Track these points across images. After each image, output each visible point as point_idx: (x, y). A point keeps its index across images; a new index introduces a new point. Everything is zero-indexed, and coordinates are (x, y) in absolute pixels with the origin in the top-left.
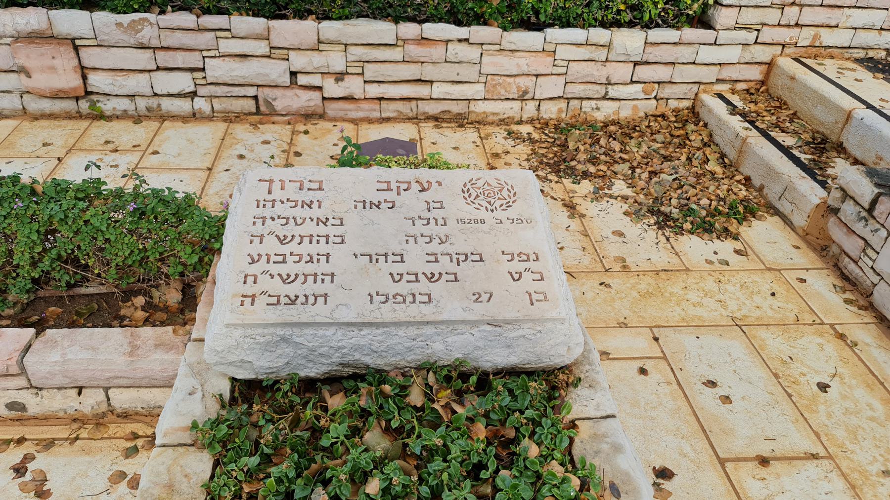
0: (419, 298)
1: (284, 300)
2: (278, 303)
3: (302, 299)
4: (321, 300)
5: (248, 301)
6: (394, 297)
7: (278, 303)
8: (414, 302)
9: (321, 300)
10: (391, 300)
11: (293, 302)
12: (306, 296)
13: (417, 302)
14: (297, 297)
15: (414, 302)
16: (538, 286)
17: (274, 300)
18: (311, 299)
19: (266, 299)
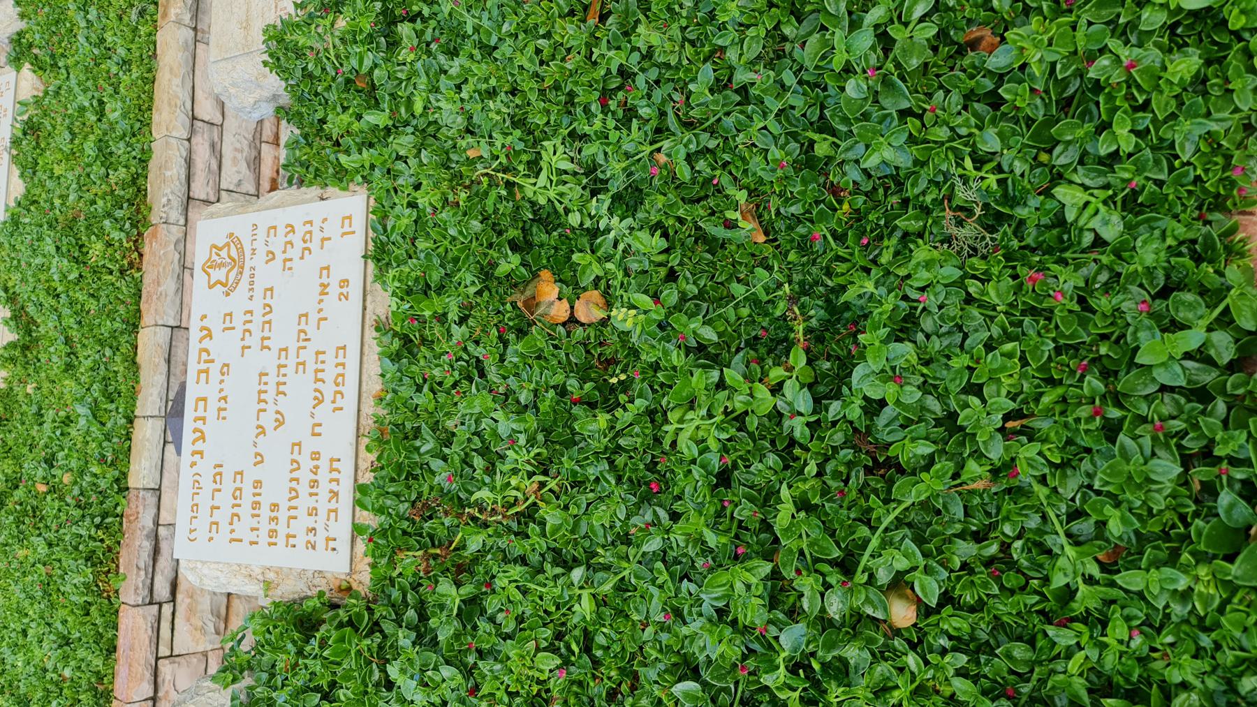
0: (340, 360)
1: (333, 505)
2: (335, 511)
3: (334, 486)
4: (335, 465)
5: (332, 544)
6: (337, 385)
7: (335, 511)
8: (343, 365)
9: (335, 465)
10: (340, 388)
11: (336, 494)
12: (331, 481)
13: (342, 360)
14: (331, 491)
15: (343, 365)
17: (333, 514)
18: (335, 475)
19: (331, 522)
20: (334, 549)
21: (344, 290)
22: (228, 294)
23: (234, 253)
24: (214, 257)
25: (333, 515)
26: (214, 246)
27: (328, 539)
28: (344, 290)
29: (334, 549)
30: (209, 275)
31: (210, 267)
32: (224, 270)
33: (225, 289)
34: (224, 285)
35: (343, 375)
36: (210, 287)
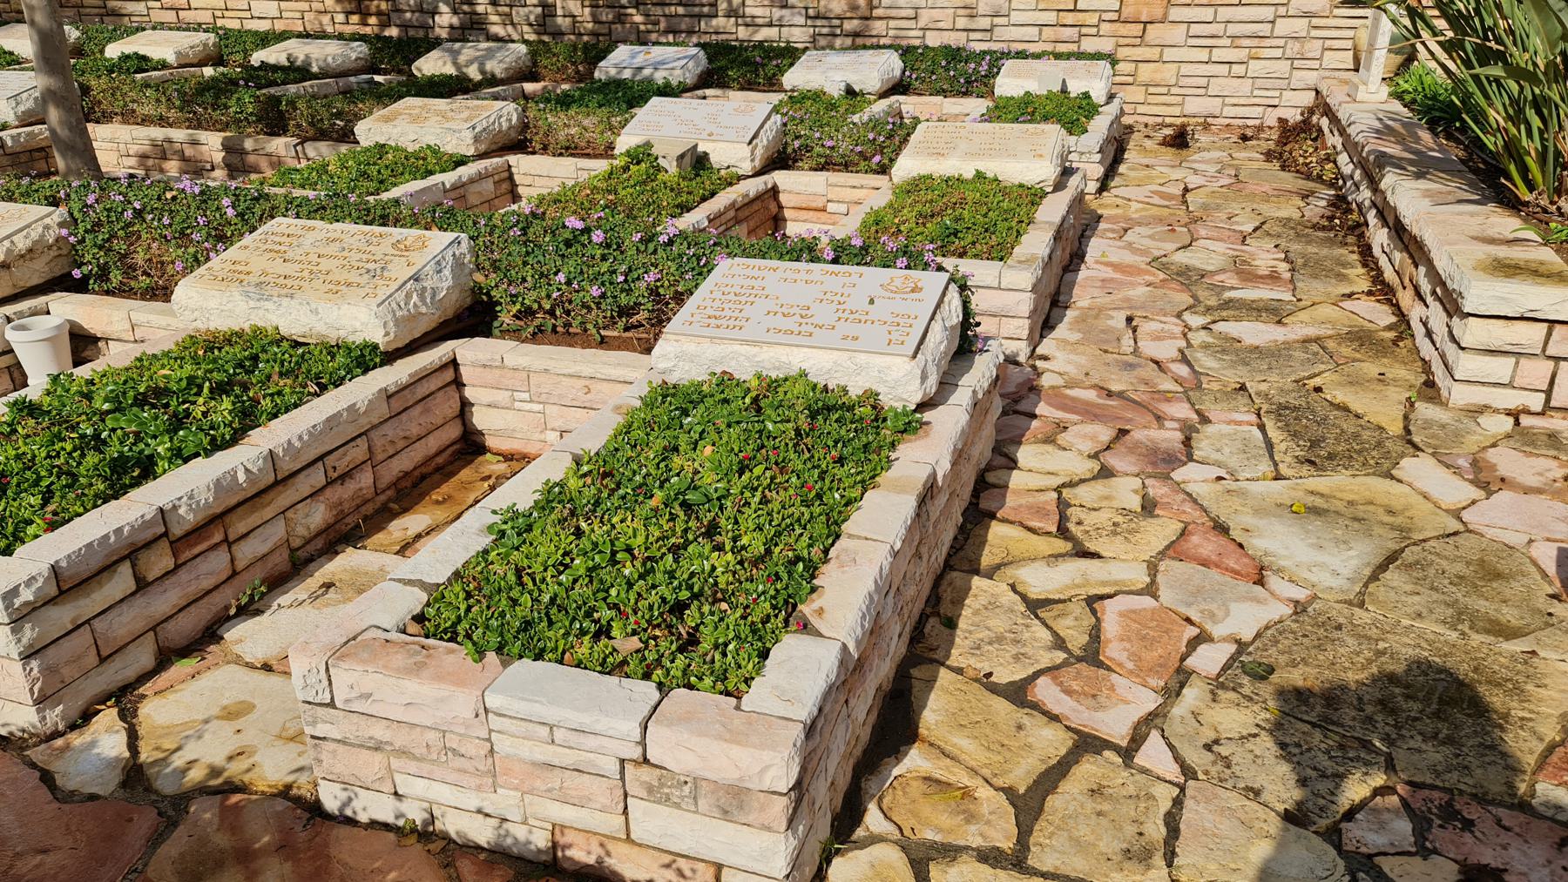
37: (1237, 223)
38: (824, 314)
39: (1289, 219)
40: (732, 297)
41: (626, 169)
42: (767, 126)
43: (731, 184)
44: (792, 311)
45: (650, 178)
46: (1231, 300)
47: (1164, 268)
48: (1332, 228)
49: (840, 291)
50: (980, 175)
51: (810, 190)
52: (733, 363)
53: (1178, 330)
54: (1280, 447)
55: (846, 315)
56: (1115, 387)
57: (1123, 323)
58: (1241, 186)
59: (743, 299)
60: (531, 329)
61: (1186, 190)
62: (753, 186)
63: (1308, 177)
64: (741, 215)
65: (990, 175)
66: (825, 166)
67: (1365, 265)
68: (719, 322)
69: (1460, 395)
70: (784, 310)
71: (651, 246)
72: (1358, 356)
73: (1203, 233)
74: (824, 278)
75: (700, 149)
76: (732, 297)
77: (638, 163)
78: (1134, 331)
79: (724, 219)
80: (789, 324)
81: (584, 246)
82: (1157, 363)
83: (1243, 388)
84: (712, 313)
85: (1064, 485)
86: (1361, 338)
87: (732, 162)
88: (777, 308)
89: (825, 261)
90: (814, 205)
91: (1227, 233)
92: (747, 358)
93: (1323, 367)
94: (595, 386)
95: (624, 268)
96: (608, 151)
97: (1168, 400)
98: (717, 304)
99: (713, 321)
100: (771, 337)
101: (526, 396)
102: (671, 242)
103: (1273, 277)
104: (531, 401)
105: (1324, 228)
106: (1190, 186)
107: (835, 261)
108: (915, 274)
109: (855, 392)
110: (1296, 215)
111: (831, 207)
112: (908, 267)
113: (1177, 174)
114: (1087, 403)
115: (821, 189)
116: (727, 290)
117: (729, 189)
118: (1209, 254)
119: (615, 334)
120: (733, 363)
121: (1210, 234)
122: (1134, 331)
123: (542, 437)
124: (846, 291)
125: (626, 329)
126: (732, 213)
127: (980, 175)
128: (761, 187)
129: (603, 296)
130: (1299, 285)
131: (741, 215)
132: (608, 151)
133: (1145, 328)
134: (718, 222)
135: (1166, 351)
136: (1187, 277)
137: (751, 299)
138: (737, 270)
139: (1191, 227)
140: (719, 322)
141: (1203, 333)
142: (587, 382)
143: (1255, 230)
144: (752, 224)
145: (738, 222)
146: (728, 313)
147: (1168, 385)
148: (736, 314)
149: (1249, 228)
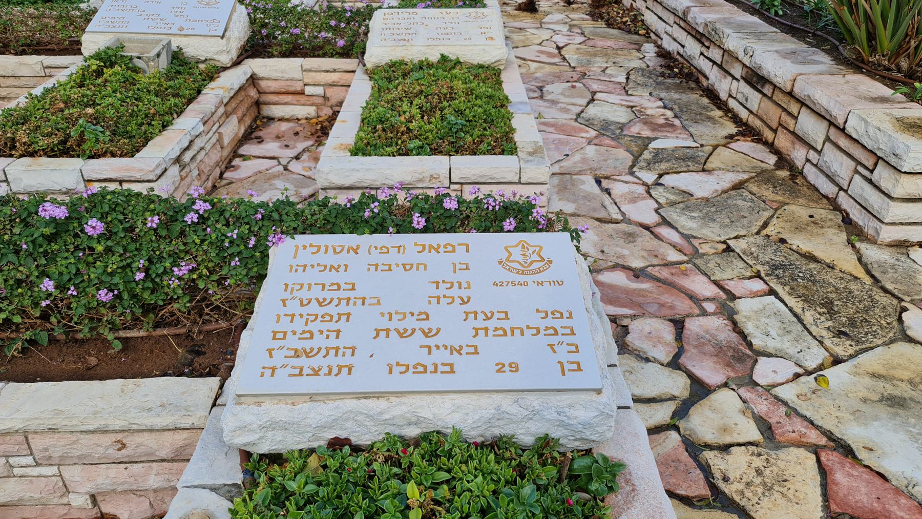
0: (441, 368)
7: (301, 374)
8: (436, 371)
11: (316, 373)
15: (436, 371)
16: (574, 357)
20: (262, 376)
21: (507, 368)
22: (500, 262)
23: (535, 266)
24: (531, 250)
25: (297, 371)
26: (541, 248)
27: (273, 369)
28: (507, 368)
29: (262, 376)
30: (517, 246)
31: (523, 246)
32: (520, 259)
33: (504, 260)
34: (507, 260)
35: (425, 372)
36: (506, 248)
37: (611, 75)
38: (452, 325)
39: (642, 69)
40: (314, 308)
41: (99, 73)
42: (234, 18)
43: (212, 79)
44: (410, 323)
45: (129, 82)
46: (657, 152)
47: (589, 123)
48: (675, 76)
49: (454, 278)
50: (444, 58)
51: (287, 76)
52: (349, 425)
53: (641, 190)
54: (808, 317)
55: (480, 323)
56: (637, 264)
57: (596, 189)
58: (591, 43)
59: (332, 309)
60: (19, 345)
61: (559, 48)
62: (233, 79)
63: (629, 32)
64: (229, 109)
65: (453, 57)
66: (294, 50)
67: (719, 108)
68: (316, 362)
69: (888, 234)
70: (394, 324)
71: (177, 227)
72: (788, 201)
73: (595, 87)
74: (426, 257)
75: (174, 47)
76: (314, 308)
77: (112, 65)
78: (609, 194)
79: (215, 118)
80: (411, 351)
81: (76, 236)
82: (647, 228)
83: (729, 249)
84: (300, 345)
85: (675, 415)
86: (763, 176)
87: (209, 56)
88: (384, 323)
89: (415, 231)
90: (292, 89)
91: (611, 85)
92: (371, 417)
93: (767, 214)
94: (132, 441)
95: (142, 262)
96: (74, 48)
97: (685, 273)
98: (299, 325)
99: (303, 361)
100: (398, 382)
101: (29, 460)
102: (203, 219)
103: (669, 125)
104: (38, 465)
105: (669, 77)
106: (561, 45)
107: (425, 230)
108: (532, 238)
109: (527, 439)
110: (644, 66)
111: (309, 90)
112: (517, 230)
113: (544, 34)
114: (627, 291)
115: (298, 75)
116: (304, 294)
117: (212, 84)
118: (611, 109)
119: (142, 333)
120: (349, 425)
121: (601, 88)
122: (609, 194)
123: (65, 500)
124: (463, 276)
125: (157, 326)
126: (221, 110)
127: (444, 58)
128: (243, 80)
129: (119, 297)
130: (691, 130)
131: (229, 109)
132: (74, 48)
133: (618, 189)
134: (210, 123)
135: (644, 212)
136: (608, 131)
137: (343, 308)
138: (305, 257)
139: (584, 81)
140: (316, 362)
141: (661, 189)
142: (119, 437)
143: (628, 78)
144: (240, 113)
145: (227, 115)
146: (319, 341)
147: (674, 256)
148: (333, 342)
149: (623, 79)
